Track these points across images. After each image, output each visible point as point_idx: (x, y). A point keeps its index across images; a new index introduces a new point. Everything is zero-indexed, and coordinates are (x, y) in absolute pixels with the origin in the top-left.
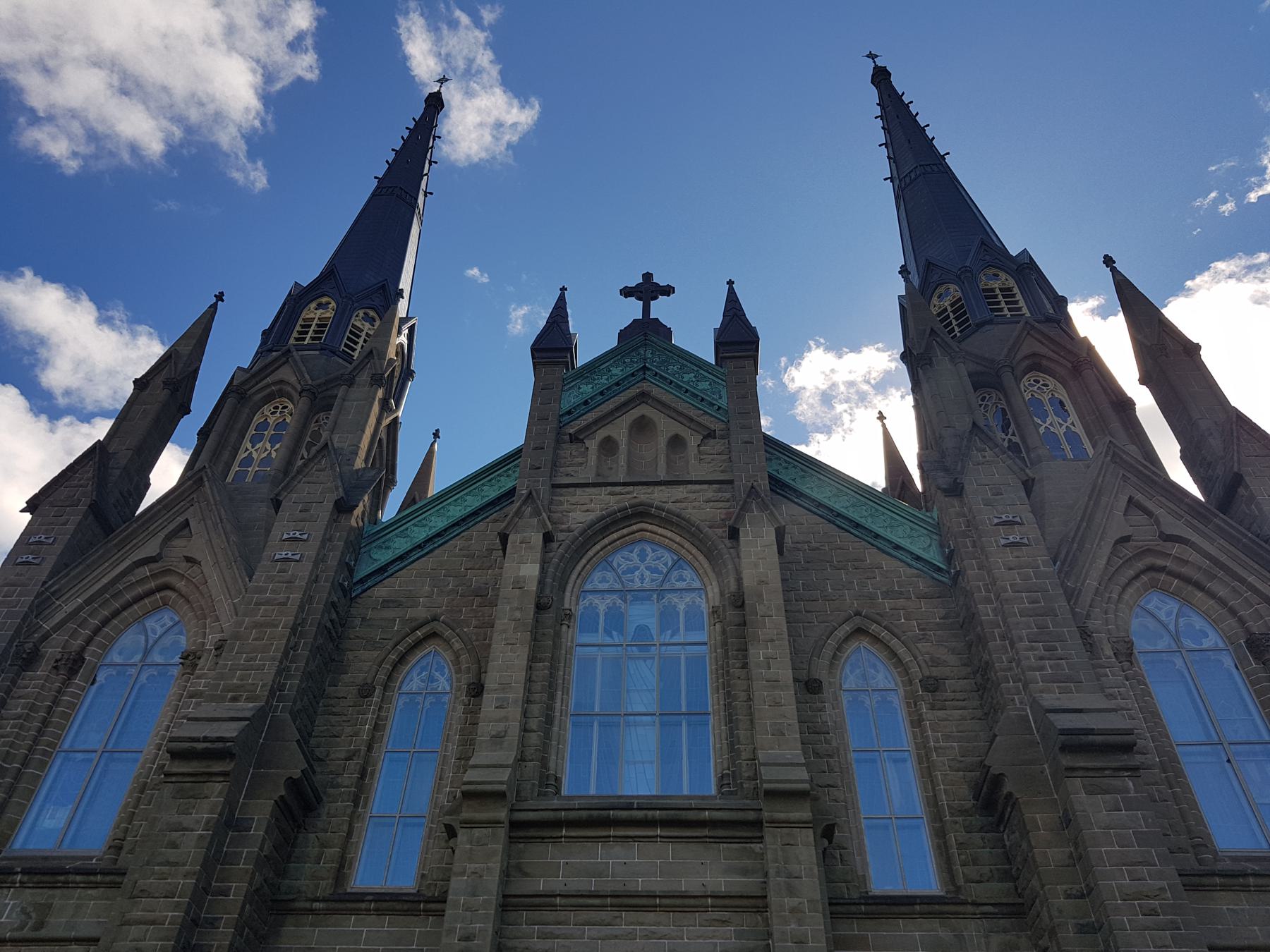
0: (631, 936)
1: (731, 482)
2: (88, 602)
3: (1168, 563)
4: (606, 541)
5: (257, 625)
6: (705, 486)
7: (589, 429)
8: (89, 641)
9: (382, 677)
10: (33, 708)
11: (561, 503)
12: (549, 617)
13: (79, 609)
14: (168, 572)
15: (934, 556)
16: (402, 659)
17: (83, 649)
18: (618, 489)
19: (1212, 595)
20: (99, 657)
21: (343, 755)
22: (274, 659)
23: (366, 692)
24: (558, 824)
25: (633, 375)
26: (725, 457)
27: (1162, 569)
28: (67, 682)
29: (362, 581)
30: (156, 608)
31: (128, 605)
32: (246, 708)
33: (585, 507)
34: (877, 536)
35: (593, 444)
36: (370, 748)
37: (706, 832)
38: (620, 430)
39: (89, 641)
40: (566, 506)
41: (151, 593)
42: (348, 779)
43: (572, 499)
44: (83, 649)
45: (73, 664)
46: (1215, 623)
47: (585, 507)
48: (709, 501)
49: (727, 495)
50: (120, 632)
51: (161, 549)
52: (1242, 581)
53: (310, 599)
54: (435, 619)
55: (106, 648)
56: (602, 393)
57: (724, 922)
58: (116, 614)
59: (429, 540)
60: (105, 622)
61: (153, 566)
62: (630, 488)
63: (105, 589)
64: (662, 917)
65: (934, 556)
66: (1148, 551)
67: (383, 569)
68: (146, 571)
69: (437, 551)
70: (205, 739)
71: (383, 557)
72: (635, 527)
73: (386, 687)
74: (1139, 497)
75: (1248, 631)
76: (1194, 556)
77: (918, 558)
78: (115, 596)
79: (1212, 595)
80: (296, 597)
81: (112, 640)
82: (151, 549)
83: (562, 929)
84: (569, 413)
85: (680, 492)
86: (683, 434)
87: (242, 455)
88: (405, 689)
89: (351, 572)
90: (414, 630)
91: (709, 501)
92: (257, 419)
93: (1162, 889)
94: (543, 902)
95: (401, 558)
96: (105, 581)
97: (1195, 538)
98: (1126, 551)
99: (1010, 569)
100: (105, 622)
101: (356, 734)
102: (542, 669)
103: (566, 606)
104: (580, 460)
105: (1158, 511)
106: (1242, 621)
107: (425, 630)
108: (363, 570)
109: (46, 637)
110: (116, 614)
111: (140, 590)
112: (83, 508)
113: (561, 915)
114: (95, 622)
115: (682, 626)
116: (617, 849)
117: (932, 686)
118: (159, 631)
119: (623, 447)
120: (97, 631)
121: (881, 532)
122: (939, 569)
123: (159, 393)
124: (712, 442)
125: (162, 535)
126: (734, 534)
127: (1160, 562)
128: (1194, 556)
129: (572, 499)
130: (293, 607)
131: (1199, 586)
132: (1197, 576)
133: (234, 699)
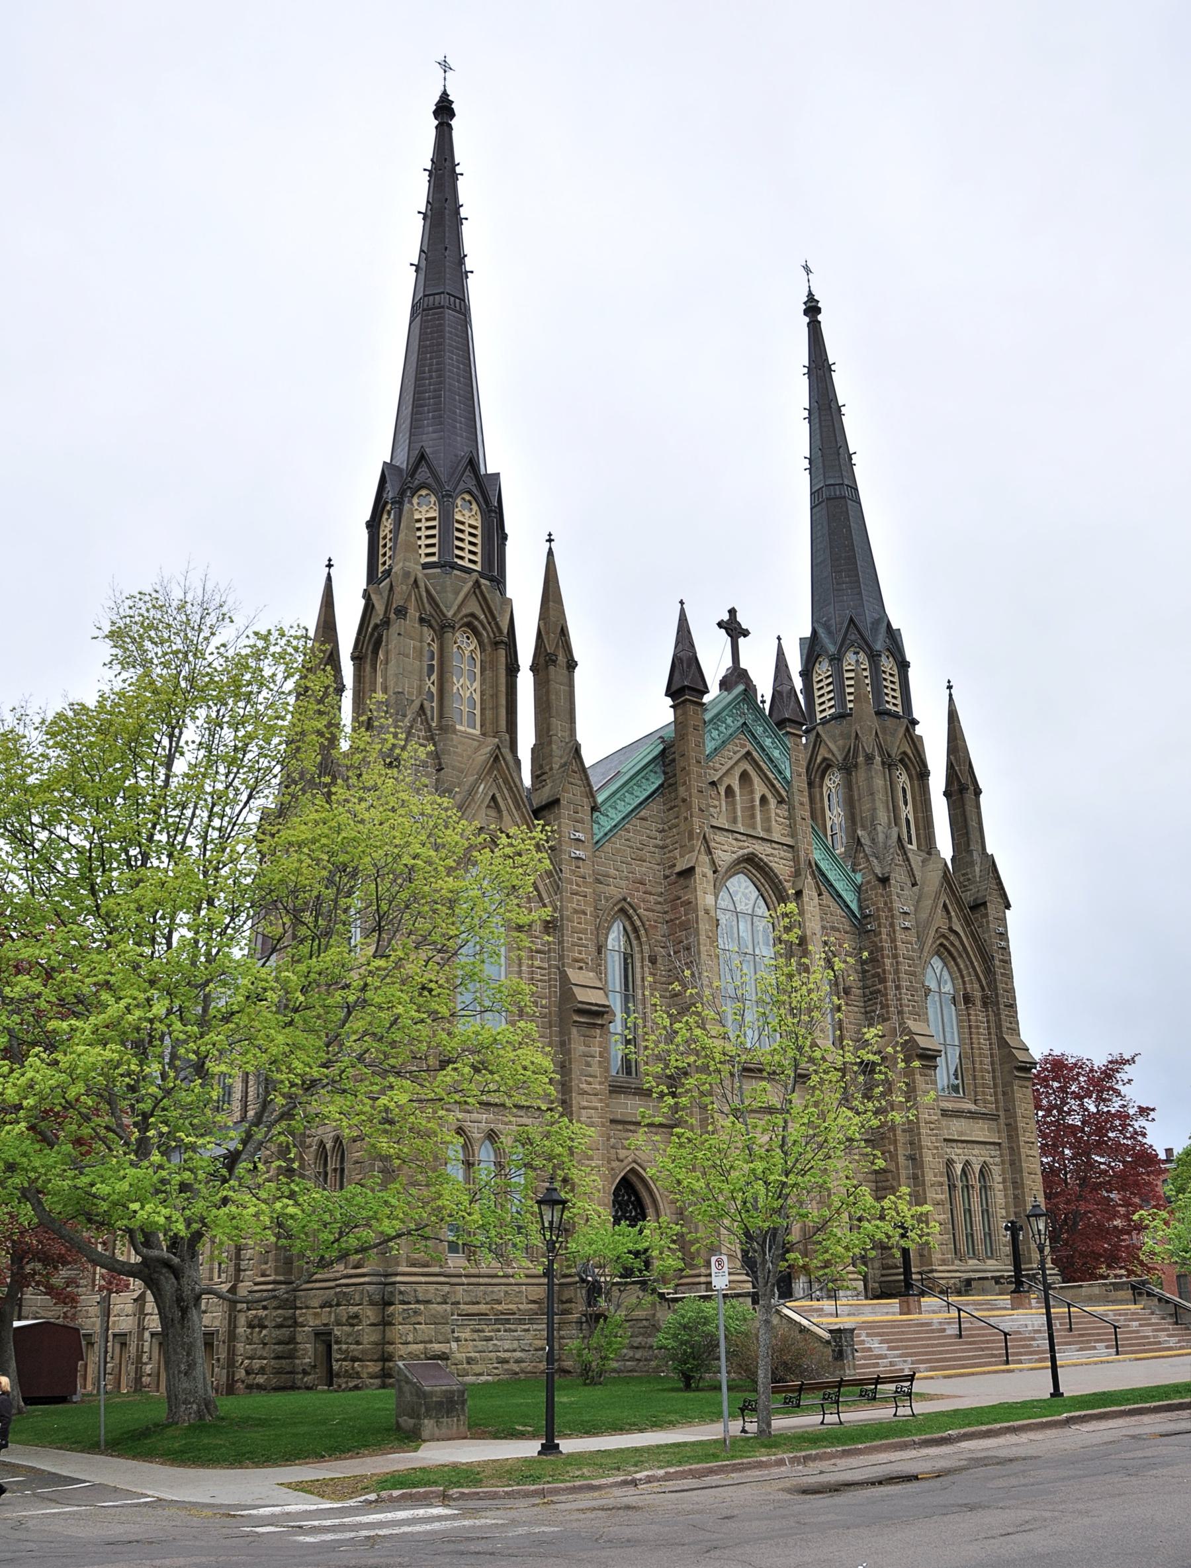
5: (576, 911)
15: (854, 906)
18: (739, 836)
19: (957, 965)
26: (787, 822)
34: (831, 885)
43: (717, 838)
49: (790, 856)
52: (972, 963)
62: (744, 838)
65: (854, 906)
70: (596, 1005)
75: (965, 989)
76: (957, 943)
77: (848, 907)
79: (957, 965)
97: (962, 934)
105: (953, 914)
106: (964, 983)
107: (619, 906)
117: (847, 991)
121: (834, 883)
122: (855, 916)
127: (945, 942)
128: (957, 943)
131: (954, 959)
132: (956, 954)
133: (581, 968)
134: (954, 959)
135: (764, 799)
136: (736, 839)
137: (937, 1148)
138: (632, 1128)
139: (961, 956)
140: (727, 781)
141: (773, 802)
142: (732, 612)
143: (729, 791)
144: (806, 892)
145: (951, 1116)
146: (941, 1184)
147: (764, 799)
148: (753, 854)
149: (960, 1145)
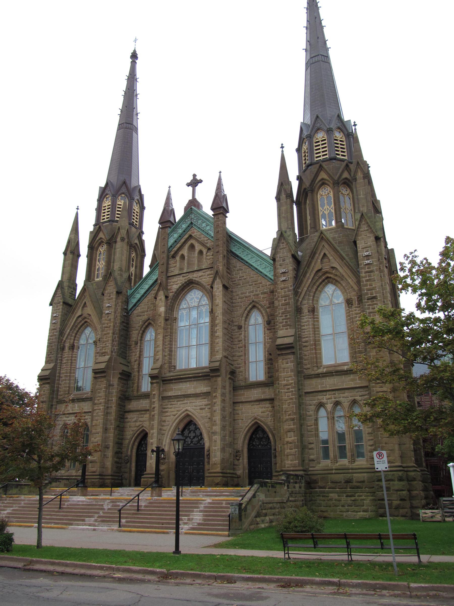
0: (187, 403)
1: (212, 267)
2: (71, 330)
3: (332, 276)
4: (184, 292)
6: (207, 270)
7: (176, 253)
8: (74, 340)
9: (139, 338)
10: (68, 360)
11: (170, 282)
12: (169, 322)
13: (69, 332)
14: (85, 318)
16: (144, 332)
17: (74, 342)
19: (342, 285)
20: (78, 343)
21: (134, 361)
22: (110, 343)
23: (136, 343)
24: (172, 380)
25: (189, 226)
27: (330, 277)
28: (73, 352)
29: (131, 309)
30: (86, 328)
31: (79, 329)
32: (107, 358)
33: (176, 283)
35: (178, 258)
36: (140, 357)
37: (202, 378)
38: (185, 251)
39: (74, 340)
40: (172, 283)
41: (83, 324)
42: (136, 367)
44: (74, 342)
45: (72, 347)
46: (343, 293)
47: (176, 283)
48: (208, 275)
50: (80, 336)
51: (82, 312)
53: (116, 323)
54: (149, 319)
55: (78, 340)
56: (180, 236)
57: (205, 398)
58: (78, 331)
59: (145, 293)
60: (76, 334)
61: (82, 317)
62: (187, 274)
63: (73, 326)
64: (193, 398)
66: (327, 272)
67: (135, 305)
68: (80, 319)
69: (148, 296)
71: (134, 301)
72: (191, 286)
73: (141, 340)
74: (327, 253)
78: (76, 326)
80: (112, 324)
81: (79, 338)
82: (79, 313)
83: (173, 403)
84: (171, 246)
85: (200, 273)
86: (202, 250)
87: (97, 267)
88: (146, 340)
89: (126, 309)
90: (145, 323)
91: (208, 275)
92: (98, 253)
93: (292, 383)
94: (169, 398)
95: (139, 300)
96: (72, 324)
97: (339, 267)
98: (320, 274)
99: (282, 289)
100: (76, 334)
101: (136, 355)
102: (168, 338)
103: (174, 316)
104: (174, 265)
108: (130, 306)
109: (65, 341)
110: (78, 331)
111: (81, 324)
112: (61, 303)
113: (173, 400)
114: (74, 335)
115: (204, 316)
116: (184, 384)
118: (89, 333)
119: (186, 258)
120: (75, 337)
123: (70, 256)
124: (210, 251)
125: (81, 308)
126: (212, 287)
127: (329, 275)
129: (173, 280)
130: (112, 328)
134: (340, 283)
135: (201, 252)
136: (183, 277)
137: (292, 399)
138: (143, 412)
139: (342, 280)
140: (180, 253)
141: (205, 251)
142: (194, 176)
143: (183, 257)
144: (215, 286)
145: (323, 377)
146: (293, 420)
147: (201, 252)
148: (190, 280)
149: (330, 393)
